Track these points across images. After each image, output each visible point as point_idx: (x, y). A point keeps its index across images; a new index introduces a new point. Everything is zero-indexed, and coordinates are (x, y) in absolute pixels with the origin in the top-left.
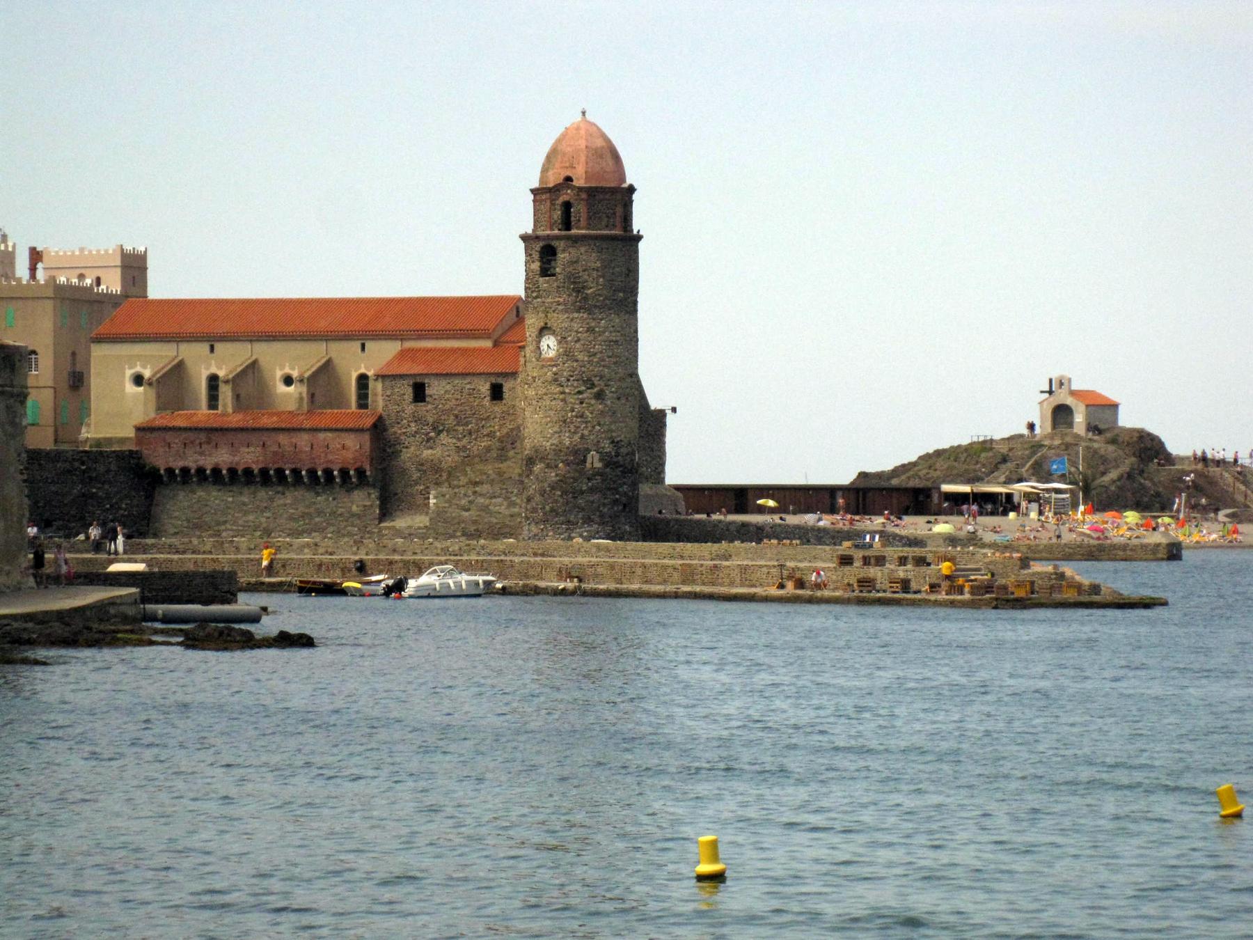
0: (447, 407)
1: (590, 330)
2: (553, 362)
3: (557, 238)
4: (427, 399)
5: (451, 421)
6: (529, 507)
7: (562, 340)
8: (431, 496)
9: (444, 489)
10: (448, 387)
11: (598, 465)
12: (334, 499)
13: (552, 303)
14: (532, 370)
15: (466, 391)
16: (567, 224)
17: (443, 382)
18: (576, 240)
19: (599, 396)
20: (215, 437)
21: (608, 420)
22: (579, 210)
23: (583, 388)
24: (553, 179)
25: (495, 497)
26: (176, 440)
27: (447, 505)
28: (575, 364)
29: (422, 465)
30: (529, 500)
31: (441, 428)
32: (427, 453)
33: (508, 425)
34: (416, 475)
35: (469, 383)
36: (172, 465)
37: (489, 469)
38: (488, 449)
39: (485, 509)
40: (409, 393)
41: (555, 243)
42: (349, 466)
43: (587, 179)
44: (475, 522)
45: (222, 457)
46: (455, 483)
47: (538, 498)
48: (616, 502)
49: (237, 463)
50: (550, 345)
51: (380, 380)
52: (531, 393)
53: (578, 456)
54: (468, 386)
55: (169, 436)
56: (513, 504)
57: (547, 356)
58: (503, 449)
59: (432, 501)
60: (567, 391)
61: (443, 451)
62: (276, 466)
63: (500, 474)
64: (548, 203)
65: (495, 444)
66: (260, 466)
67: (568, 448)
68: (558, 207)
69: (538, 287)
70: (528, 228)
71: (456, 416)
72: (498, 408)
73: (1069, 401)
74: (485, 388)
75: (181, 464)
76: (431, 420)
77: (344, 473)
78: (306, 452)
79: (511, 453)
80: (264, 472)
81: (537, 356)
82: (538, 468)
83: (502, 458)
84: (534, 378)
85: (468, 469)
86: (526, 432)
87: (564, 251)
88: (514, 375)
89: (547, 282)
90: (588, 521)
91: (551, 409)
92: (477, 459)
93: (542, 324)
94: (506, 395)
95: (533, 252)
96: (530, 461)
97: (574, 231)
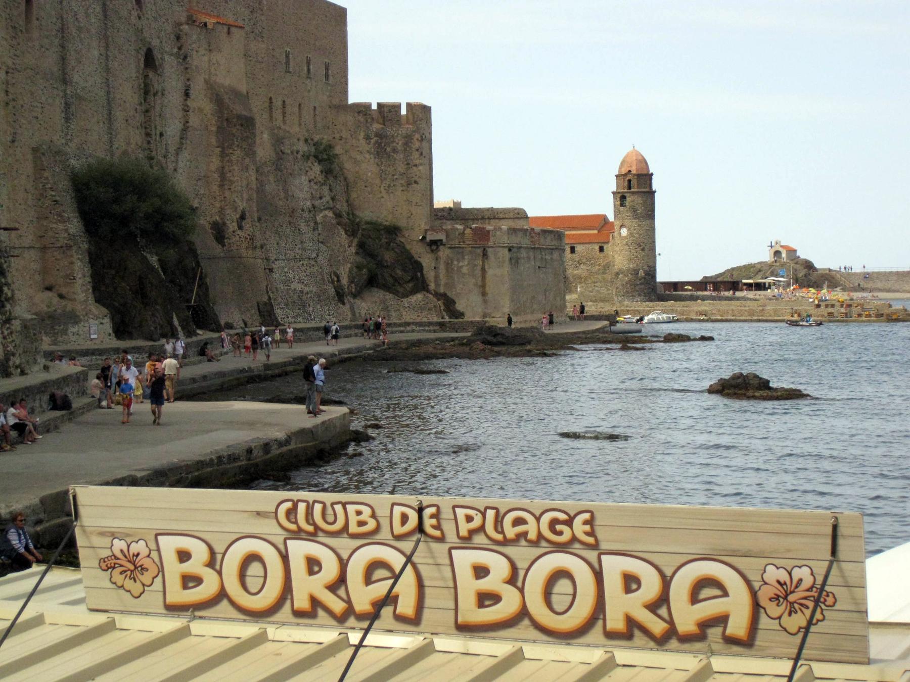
1: (639, 226)
2: (625, 238)
3: (626, 192)
5: (584, 260)
7: (629, 230)
9: (583, 285)
11: (643, 275)
14: (618, 241)
16: (630, 188)
17: (581, 246)
18: (633, 193)
19: (643, 250)
21: (646, 258)
22: (634, 182)
24: (624, 171)
30: (617, 288)
32: (576, 272)
34: (572, 280)
37: (600, 277)
38: (599, 270)
39: (598, 291)
43: (637, 170)
44: (595, 297)
48: (649, 288)
50: (624, 232)
52: (617, 249)
53: (636, 272)
56: (608, 290)
59: (579, 289)
61: (582, 271)
63: (604, 279)
65: (602, 268)
70: (615, 189)
72: (602, 255)
73: (780, 249)
74: (597, 248)
76: (577, 260)
82: (621, 276)
83: (604, 273)
86: (616, 263)
88: (607, 243)
90: (640, 295)
94: (605, 250)
96: (617, 274)
97: (632, 190)
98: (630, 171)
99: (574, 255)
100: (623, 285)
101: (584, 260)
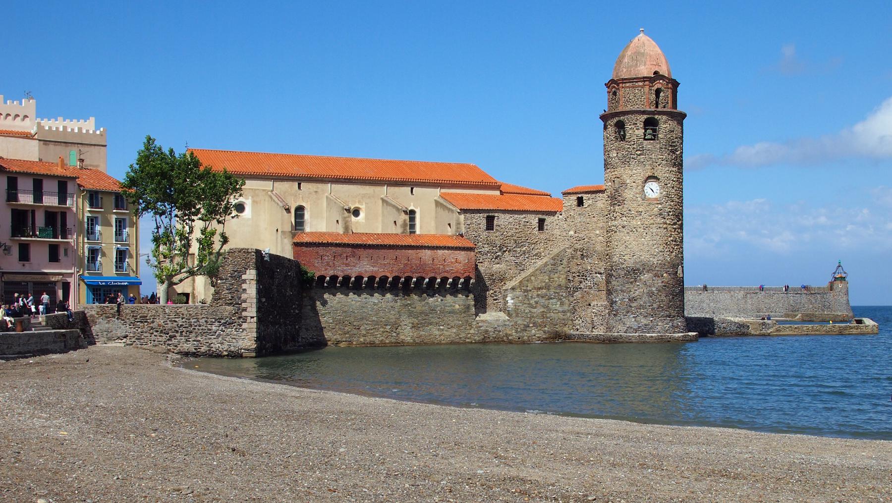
0: (510, 234)
2: (657, 201)
6: (633, 305)
8: (508, 299)
9: (518, 293)
12: (442, 300)
15: (522, 223)
17: (507, 216)
20: (361, 252)
23: (676, 221)
25: (551, 298)
26: (328, 253)
31: (505, 249)
32: (496, 267)
33: (549, 248)
34: (488, 283)
35: (525, 217)
36: (323, 273)
38: (546, 264)
40: (485, 221)
41: (656, 117)
45: (364, 267)
47: (645, 298)
49: (376, 272)
50: (653, 190)
51: (463, 211)
52: (637, 222)
54: (524, 220)
55: (321, 250)
57: (650, 196)
60: (668, 222)
62: (406, 275)
64: (647, 89)
66: (394, 275)
67: (669, 263)
68: (653, 92)
69: (643, 147)
74: (534, 220)
75: (331, 273)
76: (499, 243)
77: (456, 280)
79: (560, 268)
80: (396, 279)
81: (643, 196)
82: (646, 277)
83: (554, 271)
85: (533, 278)
87: (665, 122)
92: (538, 272)
93: (650, 174)
95: (638, 122)
96: (634, 273)
98: (655, 73)
99: (494, 235)
100: (651, 294)
101: (512, 245)
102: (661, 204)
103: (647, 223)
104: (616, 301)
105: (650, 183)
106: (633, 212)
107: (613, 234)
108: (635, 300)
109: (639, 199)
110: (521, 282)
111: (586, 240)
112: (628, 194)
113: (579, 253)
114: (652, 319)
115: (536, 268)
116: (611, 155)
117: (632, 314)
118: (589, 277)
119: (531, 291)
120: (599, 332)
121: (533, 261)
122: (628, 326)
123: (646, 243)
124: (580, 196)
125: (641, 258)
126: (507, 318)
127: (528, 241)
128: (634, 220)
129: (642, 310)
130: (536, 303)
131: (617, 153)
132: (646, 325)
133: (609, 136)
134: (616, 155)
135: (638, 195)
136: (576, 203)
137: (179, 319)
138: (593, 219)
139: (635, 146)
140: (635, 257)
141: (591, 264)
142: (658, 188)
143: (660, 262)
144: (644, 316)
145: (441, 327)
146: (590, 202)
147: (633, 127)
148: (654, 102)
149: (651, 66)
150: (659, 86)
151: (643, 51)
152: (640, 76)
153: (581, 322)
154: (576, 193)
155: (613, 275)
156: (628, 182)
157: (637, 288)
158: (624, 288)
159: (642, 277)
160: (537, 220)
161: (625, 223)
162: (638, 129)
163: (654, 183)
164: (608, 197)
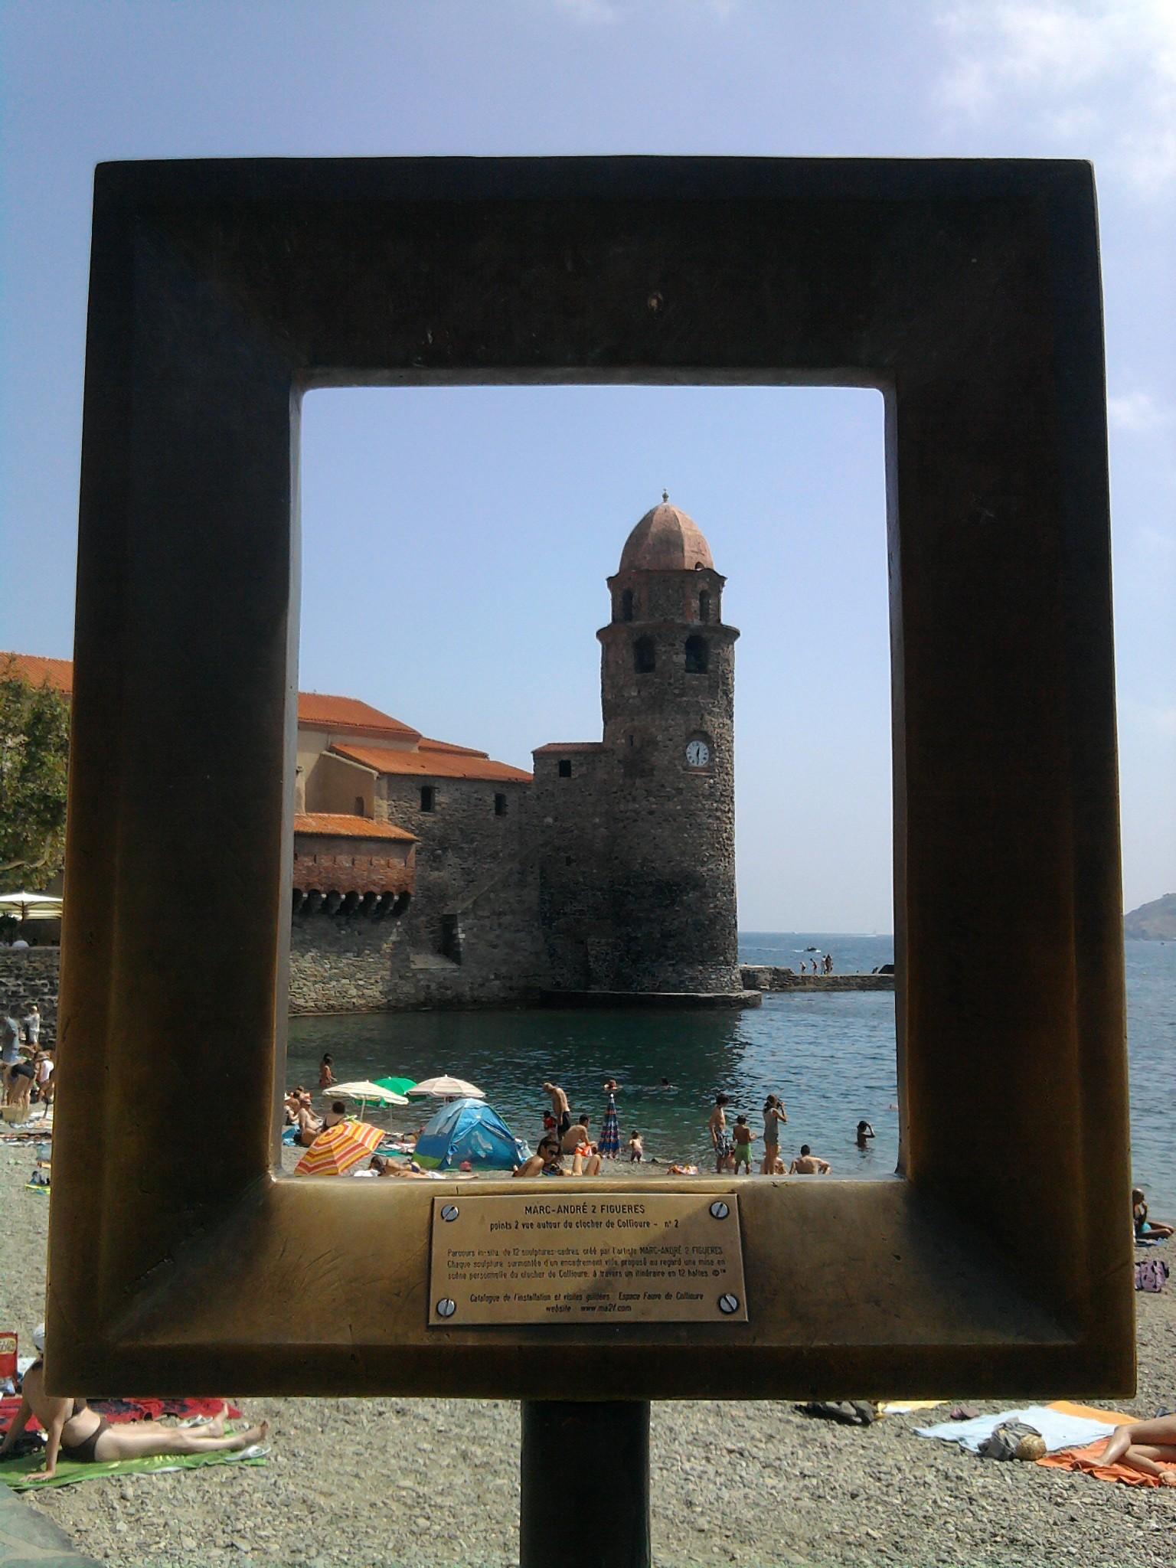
4: (437, 808)
6: (670, 944)
10: (457, 794)
13: (708, 704)
15: (473, 801)
27: (474, 941)
28: (726, 777)
29: (428, 889)
40: (419, 795)
42: (393, 890)
46: (480, 913)
54: (475, 795)
57: (695, 764)
58: (523, 874)
59: (462, 936)
60: (722, 808)
71: (461, 830)
74: (491, 799)
78: (346, 868)
79: (530, 879)
82: (691, 896)
84: (679, 791)
85: (492, 895)
89: (697, 679)
91: (708, 829)
94: (509, 809)
98: (698, 565)
102: (711, 777)
103: (693, 808)
104: (636, 938)
105: (695, 743)
106: (668, 789)
107: (628, 824)
108: (673, 936)
109: (680, 768)
110: (475, 902)
111: (576, 832)
112: (660, 759)
113: (562, 854)
114: (701, 968)
115: (496, 878)
116: (626, 695)
117: (668, 959)
118: (580, 894)
119: (489, 917)
120: (601, 989)
121: (486, 866)
122: (660, 979)
123: (690, 841)
124: (565, 758)
125: (682, 865)
126: (454, 966)
127: (480, 832)
128: (670, 803)
129: (685, 953)
130: (498, 937)
131: (639, 692)
132: (692, 979)
133: (620, 662)
134: (635, 694)
135: (677, 762)
136: (557, 771)
137: (9, 980)
138: (589, 797)
139: (672, 681)
140: (672, 864)
141: (584, 873)
142: (707, 751)
143: (710, 873)
144: (690, 964)
145: (361, 983)
146: (584, 769)
147: (668, 648)
148: (698, 612)
149: (692, 554)
150: (706, 587)
151: (676, 529)
152: (674, 567)
153: (565, 971)
154: (559, 753)
155: (629, 893)
156: (659, 738)
157: (675, 917)
158: (652, 916)
159: (685, 898)
160: (493, 798)
161: (654, 806)
162: (677, 654)
163: (701, 744)
164: (619, 761)
